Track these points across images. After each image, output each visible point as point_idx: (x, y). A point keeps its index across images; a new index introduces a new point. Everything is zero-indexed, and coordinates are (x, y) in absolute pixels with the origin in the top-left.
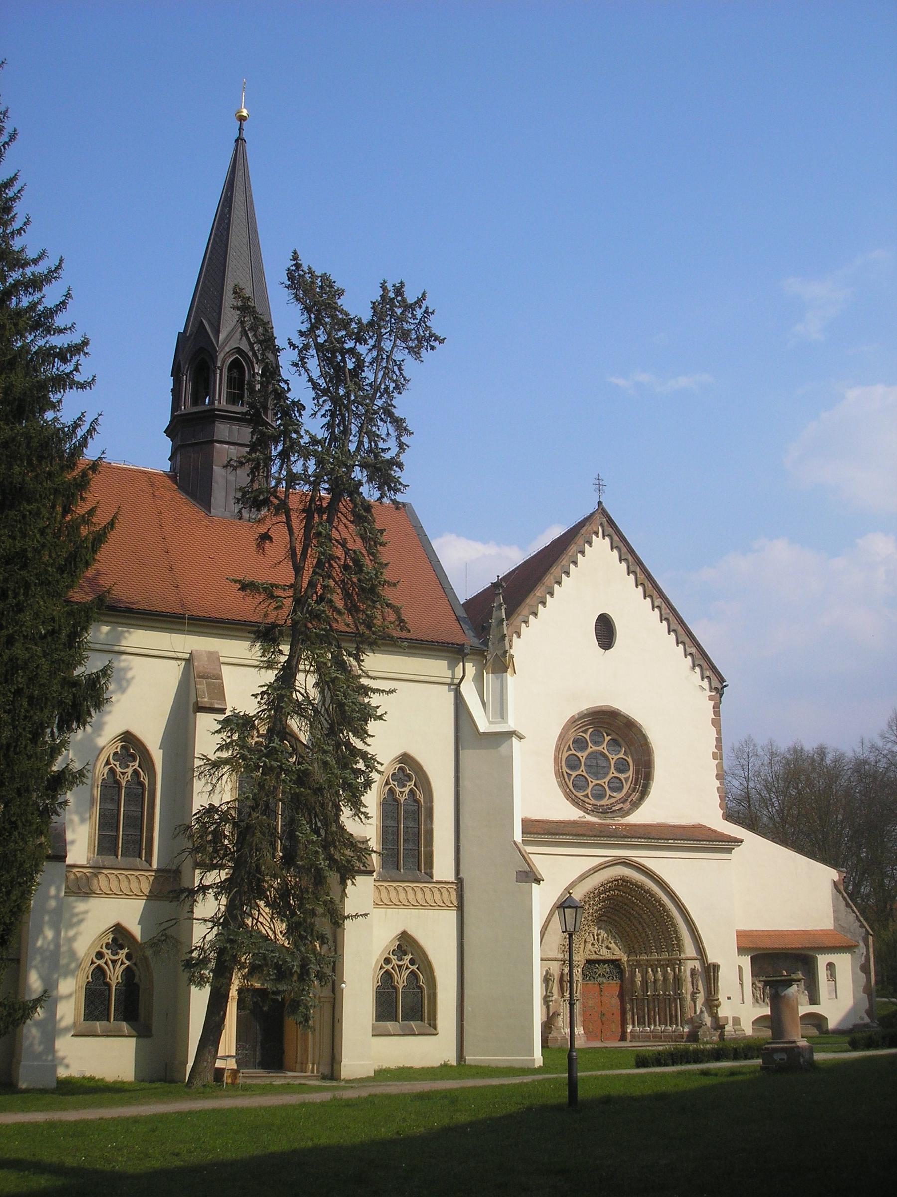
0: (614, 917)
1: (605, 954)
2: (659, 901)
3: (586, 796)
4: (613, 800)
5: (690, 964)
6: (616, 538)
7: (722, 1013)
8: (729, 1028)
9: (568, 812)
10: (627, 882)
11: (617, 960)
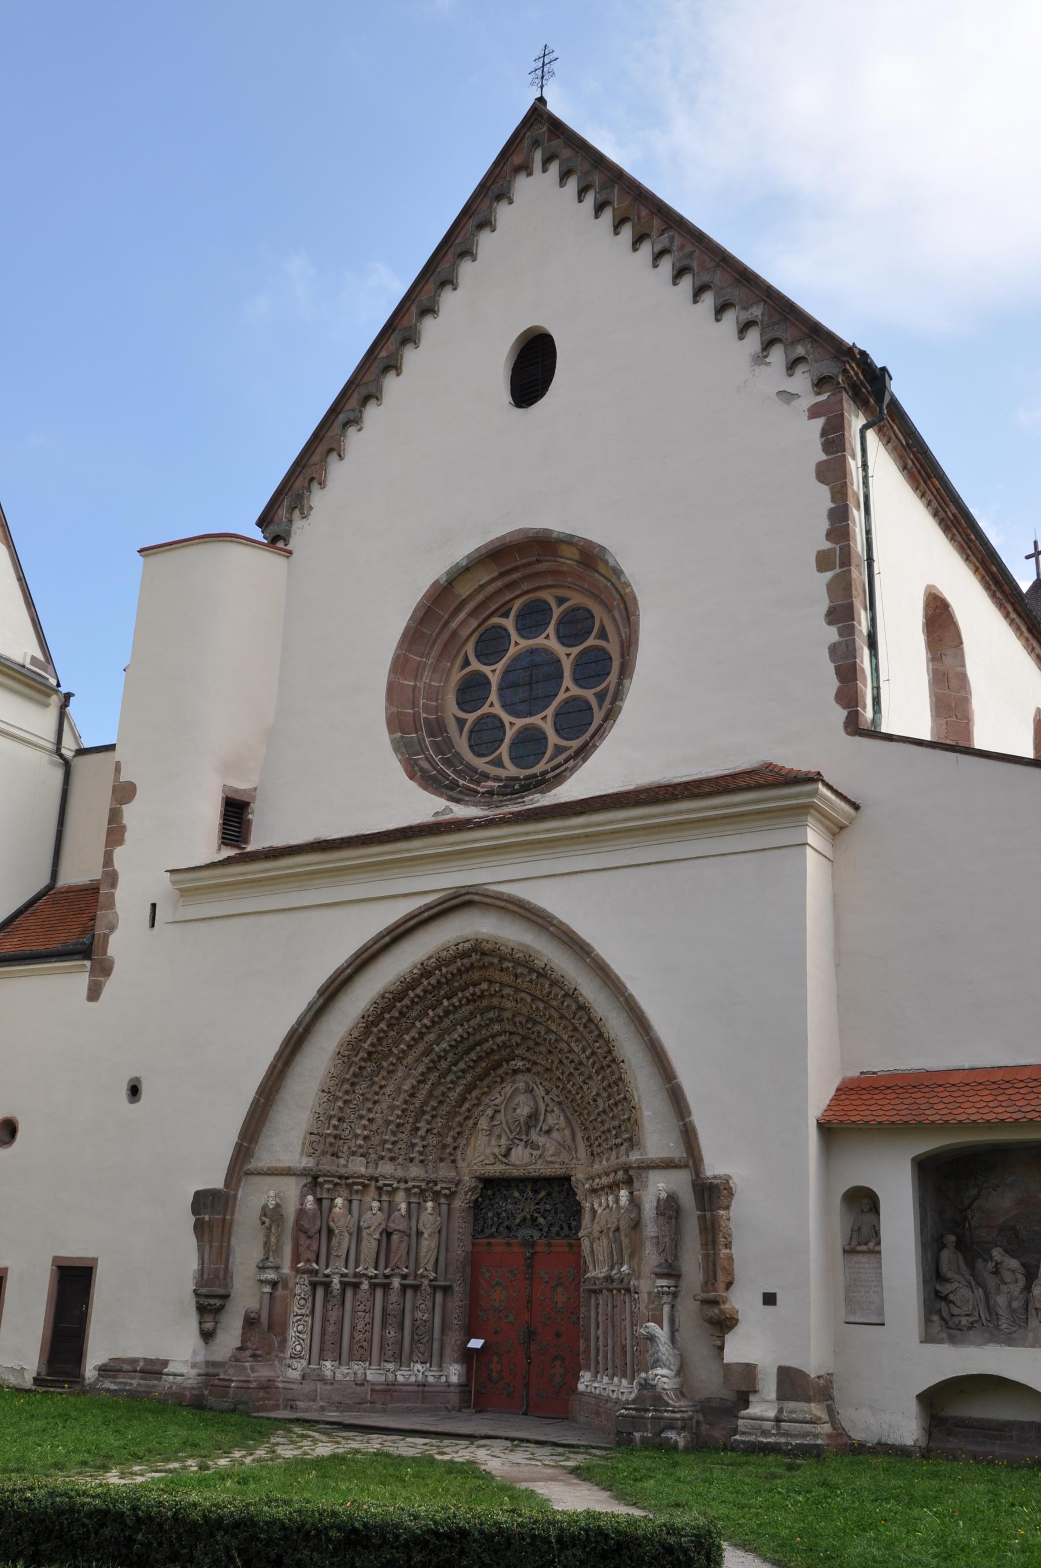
1: (522, 1160)
2: (572, 995)
3: (498, 763)
4: (561, 758)
5: (658, 1186)
6: (567, 153)
7: (738, 1349)
8: (763, 1407)
9: (425, 806)
10: (492, 953)
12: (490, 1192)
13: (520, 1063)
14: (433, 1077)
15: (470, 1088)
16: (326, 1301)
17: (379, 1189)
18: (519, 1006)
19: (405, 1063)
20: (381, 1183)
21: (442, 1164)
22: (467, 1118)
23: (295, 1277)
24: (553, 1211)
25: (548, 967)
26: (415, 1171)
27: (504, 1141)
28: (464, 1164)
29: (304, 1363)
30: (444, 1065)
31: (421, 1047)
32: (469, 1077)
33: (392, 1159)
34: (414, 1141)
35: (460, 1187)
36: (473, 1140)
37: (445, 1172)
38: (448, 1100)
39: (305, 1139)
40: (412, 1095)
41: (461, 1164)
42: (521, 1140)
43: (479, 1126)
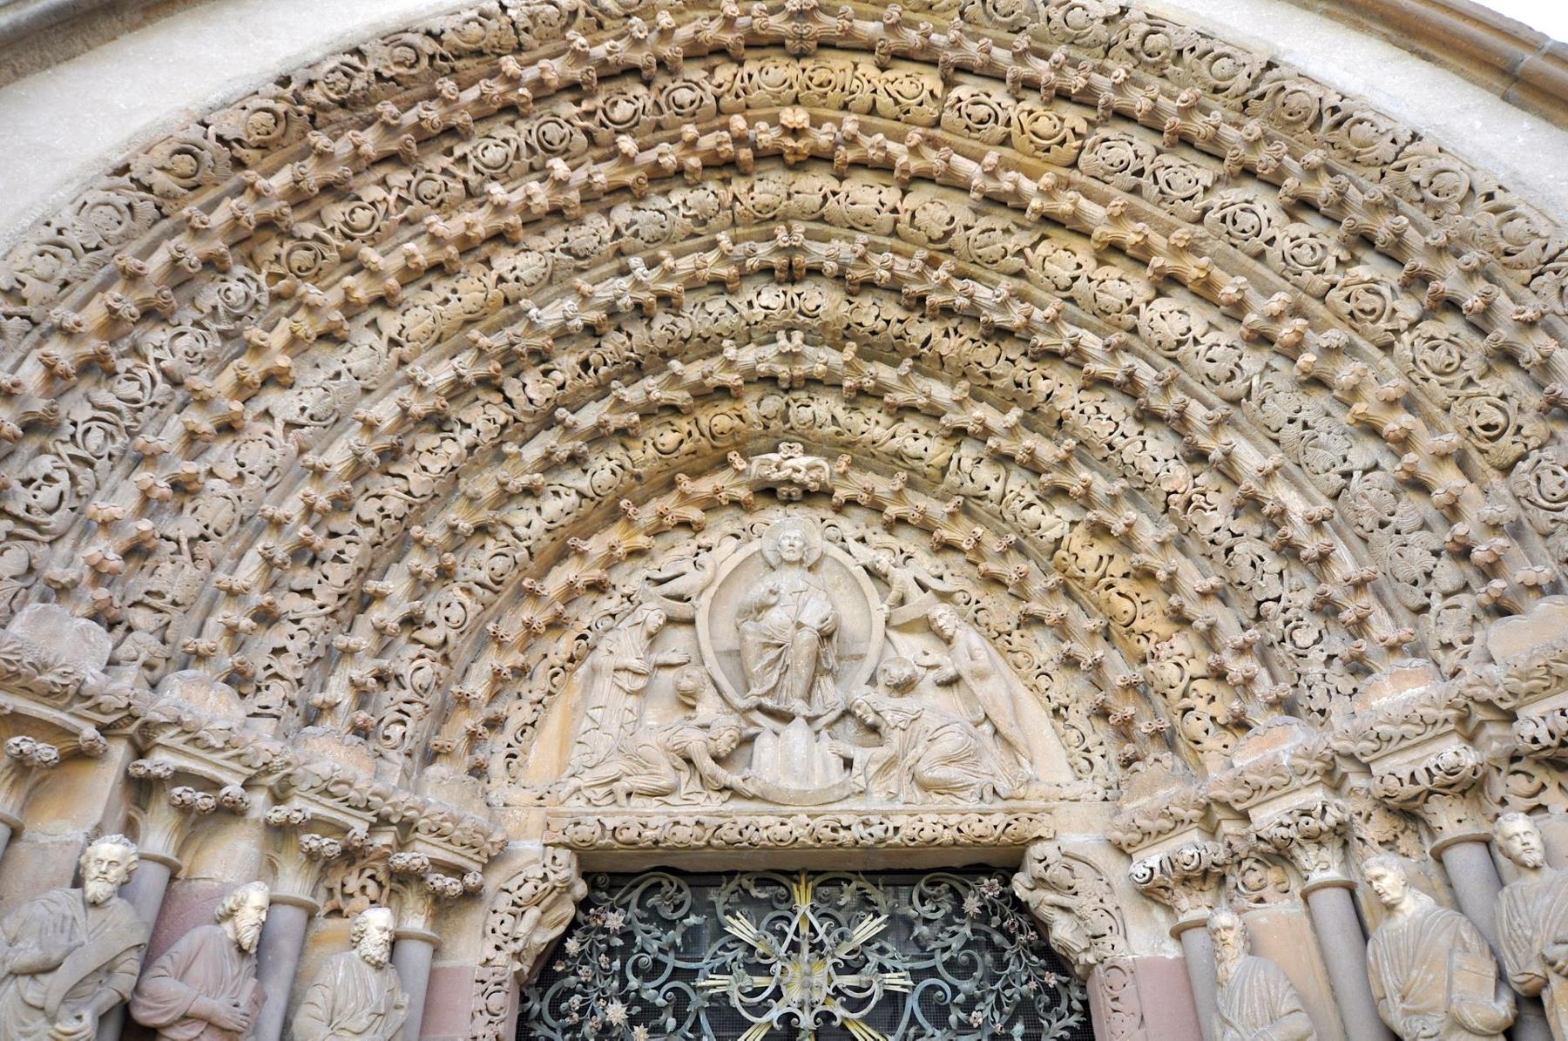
0: (871, 425)
1: (801, 786)
11: (1002, 861)
12: (615, 921)
13: (802, 461)
14: (483, 417)
15: (606, 510)
17: (142, 789)
18: (911, 201)
20: (161, 762)
21: (433, 770)
22: (557, 624)
24: (912, 1003)
25: (1133, 14)
26: (329, 754)
27: (708, 708)
28: (516, 795)
30: (535, 388)
31: (472, 288)
32: (603, 470)
33: (238, 680)
34: (341, 641)
35: (494, 880)
36: (554, 721)
37: (441, 793)
38: (505, 534)
40: (392, 454)
41: (499, 789)
42: (785, 717)
43: (600, 657)
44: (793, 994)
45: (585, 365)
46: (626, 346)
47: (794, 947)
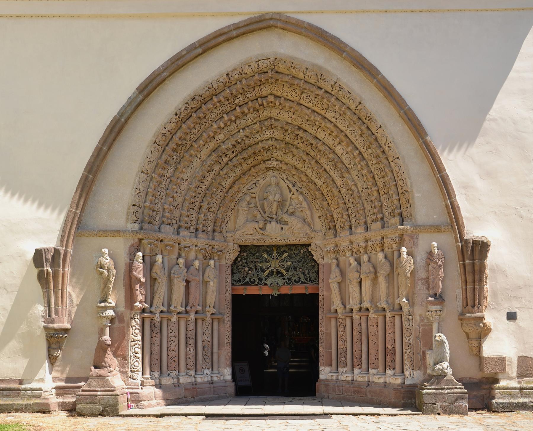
0: (288, 159)
13: (275, 163)
16: (152, 331)
19: (199, 156)
23: (130, 314)
24: (292, 267)
29: (140, 373)
39: (129, 209)
44: (273, 266)
45: (233, 152)
46: (241, 148)
47: (273, 259)
